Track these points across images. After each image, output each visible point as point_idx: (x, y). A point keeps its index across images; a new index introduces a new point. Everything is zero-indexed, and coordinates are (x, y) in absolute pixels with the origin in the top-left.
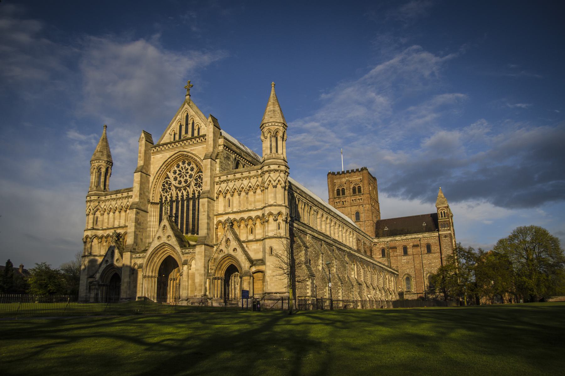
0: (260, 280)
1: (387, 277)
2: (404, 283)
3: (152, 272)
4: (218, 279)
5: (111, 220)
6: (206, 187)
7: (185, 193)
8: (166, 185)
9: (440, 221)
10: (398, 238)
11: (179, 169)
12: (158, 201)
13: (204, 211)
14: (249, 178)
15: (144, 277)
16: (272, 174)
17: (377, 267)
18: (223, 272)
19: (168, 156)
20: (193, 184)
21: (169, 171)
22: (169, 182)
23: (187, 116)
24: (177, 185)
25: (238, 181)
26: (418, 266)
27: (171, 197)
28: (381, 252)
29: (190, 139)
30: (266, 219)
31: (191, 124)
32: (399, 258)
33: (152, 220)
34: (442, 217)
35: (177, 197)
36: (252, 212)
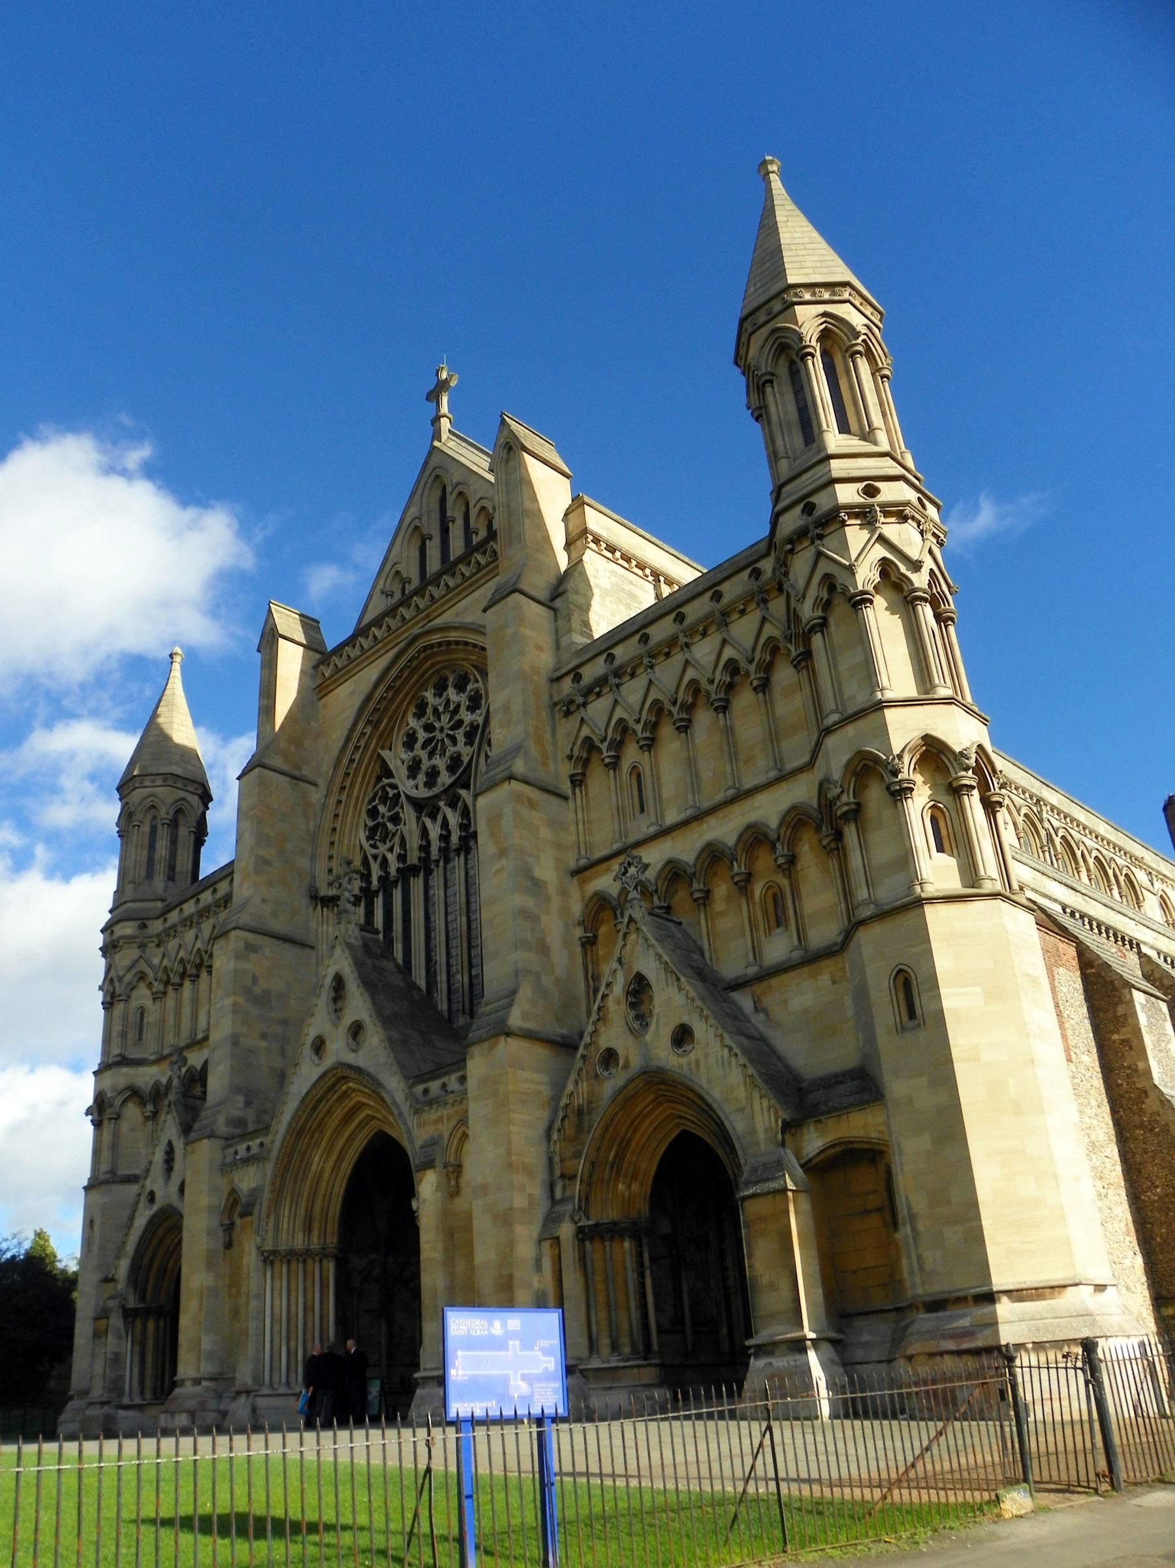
0: (867, 1212)
3: (308, 1228)
7: (454, 819)
11: (423, 720)
14: (723, 619)
18: (635, 1187)
21: (387, 745)
22: (391, 793)
24: (423, 793)
25: (668, 655)
30: (844, 798)
35: (425, 848)
36: (761, 799)
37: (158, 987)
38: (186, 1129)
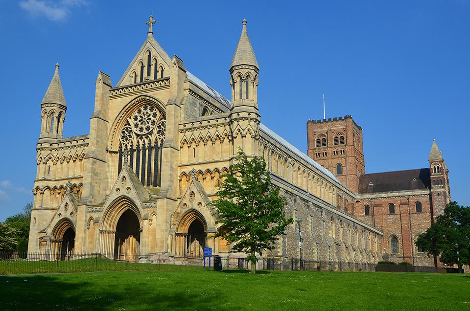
1: (370, 237)
2: (390, 245)
3: (110, 227)
4: (181, 235)
5: (65, 170)
6: (168, 135)
7: (147, 142)
8: (126, 132)
9: (433, 178)
10: (384, 195)
12: (117, 149)
13: (167, 162)
15: (101, 232)
16: (241, 123)
17: (358, 226)
19: (129, 101)
20: (155, 131)
23: (149, 57)
26: (405, 226)
27: (132, 146)
28: (364, 210)
29: (153, 83)
31: (154, 65)
32: (384, 216)
33: (110, 170)
34: (435, 172)
35: (138, 145)
37: (55, 161)
38: (72, 201)
